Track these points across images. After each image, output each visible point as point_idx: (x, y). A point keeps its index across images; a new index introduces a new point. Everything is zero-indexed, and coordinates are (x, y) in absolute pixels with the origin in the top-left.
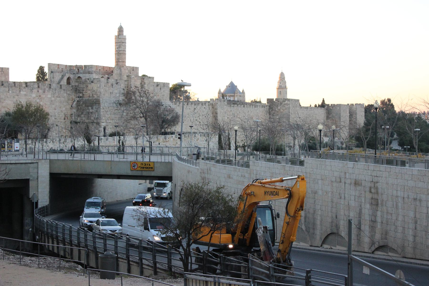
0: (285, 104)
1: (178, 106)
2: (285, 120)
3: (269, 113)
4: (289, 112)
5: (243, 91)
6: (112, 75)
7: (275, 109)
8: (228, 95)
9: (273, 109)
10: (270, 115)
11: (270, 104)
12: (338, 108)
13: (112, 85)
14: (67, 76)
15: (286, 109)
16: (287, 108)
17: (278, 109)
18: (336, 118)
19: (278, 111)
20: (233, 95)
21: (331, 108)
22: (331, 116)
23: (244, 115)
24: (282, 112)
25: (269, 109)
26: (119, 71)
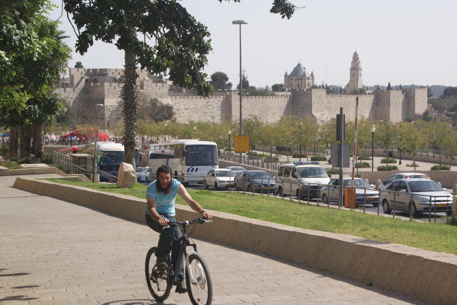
0: (308, 94)
4: (311, 102)
8: (295, 78)
12: (388, 94)
13: (115, 88)
21: (381, 94)
23: (263, 106)
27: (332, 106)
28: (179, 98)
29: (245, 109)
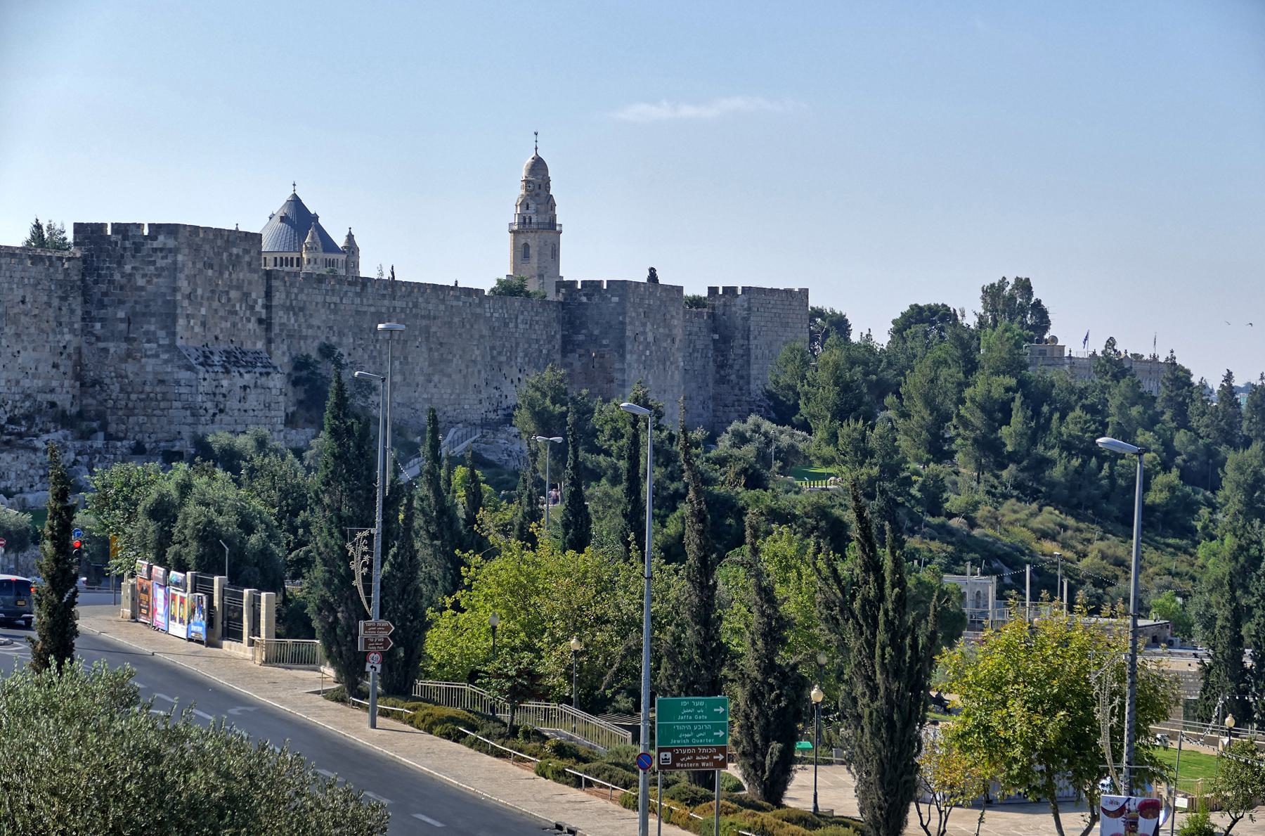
0: (155, 250)
2: (153, 328)
3: (83, 295)
4: (175, 290)
5: (350, 237)
7: (112, 275)
9: (99, 275)
10: (85, 302)
11: (89, 250)
15: (159, 276)
16: (162, 269)
17: (123, 275)
18: (606, 346)
19: (124, 281)
21: (584, 299)
22: (581, 337)
24: (142, 289)
25: (83, 275)
27: (310, 326)
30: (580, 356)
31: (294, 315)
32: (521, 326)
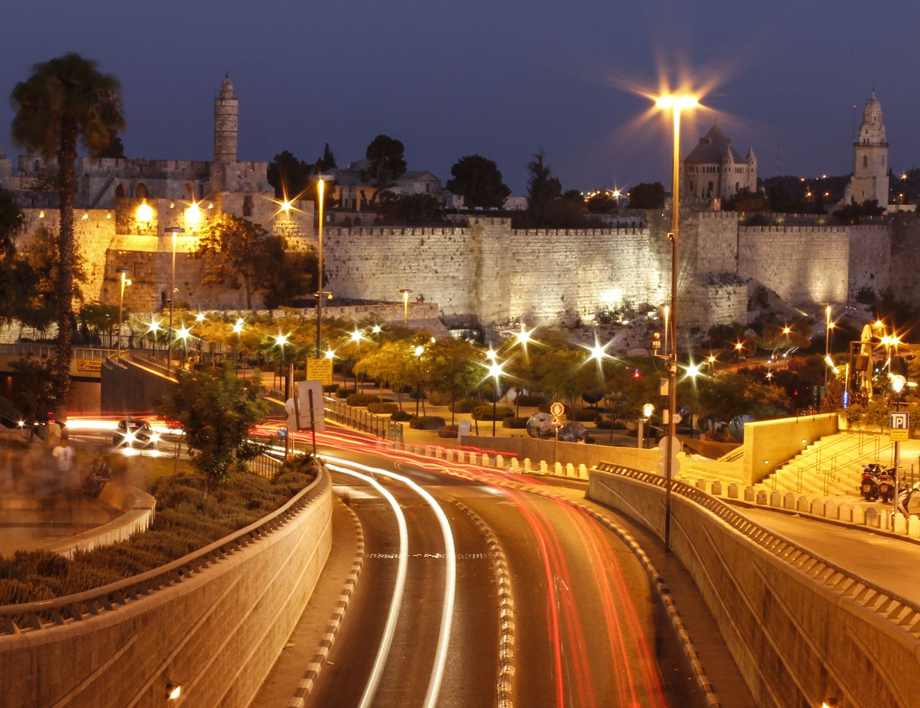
1: (377, 237)
6: (208, 180)
8: (700, 166)
14: (117, 182)
20: (716, 166)
21: (905, 224)
26: (221, 172)
28: (346, 233)
29: (518, 261)
30: (902, 256)
31: (750, 249)
32: (868, 241)
